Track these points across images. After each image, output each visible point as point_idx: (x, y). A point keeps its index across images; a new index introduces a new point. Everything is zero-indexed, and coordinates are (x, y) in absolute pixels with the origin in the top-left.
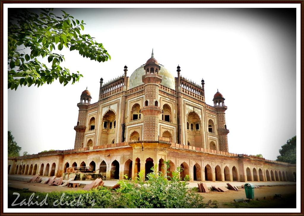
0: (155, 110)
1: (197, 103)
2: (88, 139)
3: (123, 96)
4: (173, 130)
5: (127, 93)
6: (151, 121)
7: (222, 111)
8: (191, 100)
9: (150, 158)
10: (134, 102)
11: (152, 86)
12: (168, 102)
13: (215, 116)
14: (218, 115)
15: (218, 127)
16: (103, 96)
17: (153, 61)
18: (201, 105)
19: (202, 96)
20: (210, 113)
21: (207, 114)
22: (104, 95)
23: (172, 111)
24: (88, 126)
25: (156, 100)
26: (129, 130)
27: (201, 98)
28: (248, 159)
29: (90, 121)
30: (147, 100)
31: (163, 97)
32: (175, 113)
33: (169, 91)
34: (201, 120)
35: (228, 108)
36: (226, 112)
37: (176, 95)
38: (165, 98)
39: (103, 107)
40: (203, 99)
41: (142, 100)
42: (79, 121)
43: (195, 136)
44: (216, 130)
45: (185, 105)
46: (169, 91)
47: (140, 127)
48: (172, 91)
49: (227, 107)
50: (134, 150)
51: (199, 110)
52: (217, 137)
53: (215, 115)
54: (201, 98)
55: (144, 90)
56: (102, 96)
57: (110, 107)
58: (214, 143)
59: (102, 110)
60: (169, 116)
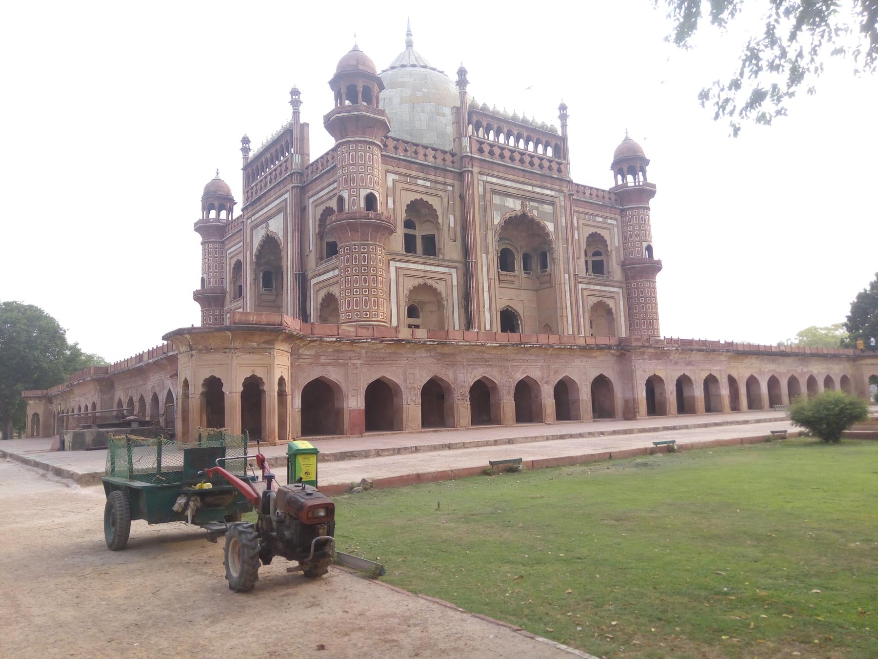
0: (362, 224)
1: (538, 183)
4: (445, 280)
6: (356, 259)
8: (516, 178)
9: (253, 377)
10: (322, 203)
11: (352, 147)
12: (426, 193)
13: (615, 219)
14: (627, 216)
15: (625, 254)
17: (354, 63)
18: (552, 189)
19: (559, 157)
20: (594, 212)
21: (582, 216)
22: (252, 188)
23: (440, 220)
24: (228, 287)
25: (369, 191)
27: (555, 166)
28: (651, 350)
29: (233, 273)
31: (402, 178)
32: (452, 225)
33: (425, 155)
34: (552, 237)
35: (658, 189)
37: (454, 167)
38: (413, 181)
40: (559, 171)
42: (205, 276)
43: (536, 291)
44: (615, 265)
45: (488, 195)
46: (425, 155)
49: (654, 186)
50: (179, 356)
51: (545, 206)
52: (619, 287)
53: (613, 216)
54: (555, 166)
57: (267, 227)
58: (608, 305)
59: (252, 235)
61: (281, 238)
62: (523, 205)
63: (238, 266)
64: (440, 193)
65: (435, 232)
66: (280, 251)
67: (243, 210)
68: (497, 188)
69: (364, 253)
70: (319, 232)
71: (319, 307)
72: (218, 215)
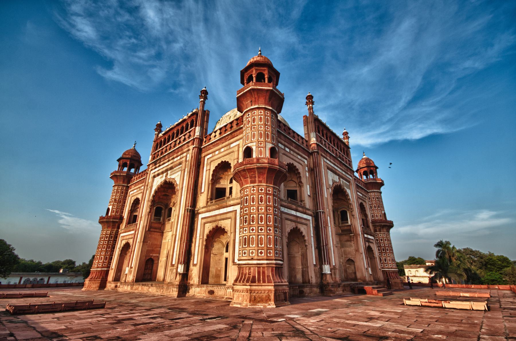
2: (124, 242)
3: (193, 149)
5: (204, 143)
7: (376, 189)
22: (158, 152)
23: (302, 180)
24: (126, 215)
26: (203, 223)
29: (132, 206)
30: (249, 145)
35: (385, 183)
36: (382, 189)
39: (154, 177)
41: (236, 153)
42: (111, 207)
47: (229, 215)
48: (301, 141)
49: (383, 181)
52: (374, 236)
59: (153, 181)
60: (296, 191)
61: (178, 183)
62: (339, 178)
63: (137, 202)
64: (302, 163)
65: (298, 189)
67: (149, 165)
68: (329, 166)
69: (270, 194)
70: (212, 179)
71: (205, 237)
72: (129, 170)
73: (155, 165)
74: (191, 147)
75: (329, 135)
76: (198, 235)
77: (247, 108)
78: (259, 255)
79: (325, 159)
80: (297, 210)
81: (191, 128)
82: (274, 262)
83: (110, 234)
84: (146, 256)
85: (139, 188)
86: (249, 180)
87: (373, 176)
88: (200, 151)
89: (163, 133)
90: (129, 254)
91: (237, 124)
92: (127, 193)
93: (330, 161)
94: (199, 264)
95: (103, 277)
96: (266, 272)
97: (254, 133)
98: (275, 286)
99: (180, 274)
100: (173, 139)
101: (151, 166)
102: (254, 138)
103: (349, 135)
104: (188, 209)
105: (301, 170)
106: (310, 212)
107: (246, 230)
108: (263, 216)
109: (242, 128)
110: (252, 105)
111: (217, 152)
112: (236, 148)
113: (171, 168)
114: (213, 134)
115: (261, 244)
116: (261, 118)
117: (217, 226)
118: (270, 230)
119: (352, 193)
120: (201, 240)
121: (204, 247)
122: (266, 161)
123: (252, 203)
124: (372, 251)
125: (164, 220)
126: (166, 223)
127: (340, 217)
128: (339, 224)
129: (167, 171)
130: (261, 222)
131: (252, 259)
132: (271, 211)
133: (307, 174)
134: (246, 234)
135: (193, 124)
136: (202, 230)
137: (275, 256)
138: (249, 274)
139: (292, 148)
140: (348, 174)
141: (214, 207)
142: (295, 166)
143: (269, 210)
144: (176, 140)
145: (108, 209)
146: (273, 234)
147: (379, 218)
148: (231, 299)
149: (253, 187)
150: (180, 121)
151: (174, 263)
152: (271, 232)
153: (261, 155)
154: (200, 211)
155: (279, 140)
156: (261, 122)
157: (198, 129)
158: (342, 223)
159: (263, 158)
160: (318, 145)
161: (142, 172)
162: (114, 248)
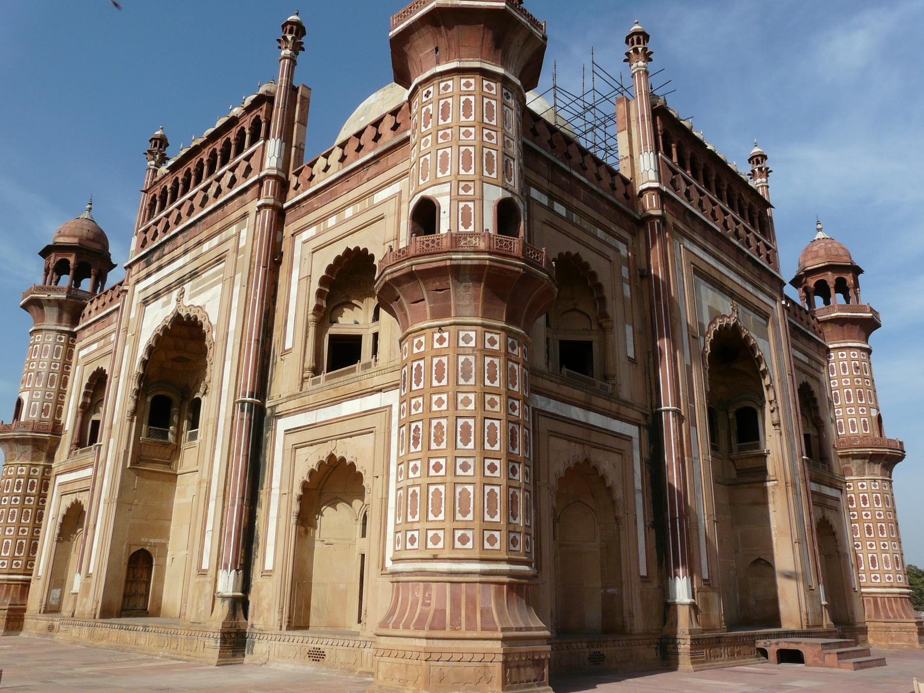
2: (67, 501)
3: (258, 212)
5: (291, 192)
16: (153, 229)
22: (156, 224)
23: (609, 310)
29: (86, 395)
30: (428, 193)
35: (883, 319)
39: (145, 302)
42: (25, 397)
43: (729, 485)
47: (367, 422)
48: (607, 180)
55: (408, 139)
56: (149, 235)
59: (142, 315)
60: (589, 344)
61: (214, 321)
63: (98, 382)
64: (610, 252)
65: (594, 338)
66: (203, 352)
67: (130, 267)
69: (493, 354)
70: (318, 308)
71: (297, 491)
73: (148, 264)
74: (253, 206)
75: (701, 161)
76: (276, 484)
77: (422, 72)
78: (458, 545)
79: (687, 244)
80: (587, 407)
81: (252, 142)
82: (505, 567)
83: (29, 477)
84: (130, 546)
85: (104, 337)
86: (427, 305)
87: (847, 298)
88: (279, 217)
89: (170, 163)
90: (81, 537)
91: (395, 127)
92: (69, 354)
93: (705, 249)
94: (278, 572)
95: (13, 599)
96: (479, 598)
97: (445, 155)
98: (504, 640)
99: (224, 598)
100: (198, 181)
101: (135, 268)
102: (444, 170)
103: (767, 164)
104: (243, 402)
105: (604, 278)
106: (633, 414)
107: (415, 469)
108: (471, 422)
109: (408, 139)
110: (438, 63)
111: (332, 221)
112: (392, 205)
113: (194, 275)
114: (322, 162)
115: (465, 513)
116: (467, 102)
117: (332, 456)
118: (493, 468)
119: (773, 351)
120: (285, 498)
121: (293, 520)
122: (482, 245)
123: (435, 383)
124: (834, 534)
125: (178, 435)
126: (184, 445)
127: (735, 428)
128: (730, 450)
129: (181, 282)
130: (466, 441)
131: (435, 558)
132: (497, 408)
133: (627, 288)
134: (418, 482)
135: (257, 132)
136: (287, 471)
137: (509, 551)
138: (424, 604)
139: (575, 203)
140: (763, 291)
141: (322, 397)
142: (586, 265)
143: (493, 403)
144: (208, 186)
145: (19, 403)
146: (503, 481)
147: (859, 431)
148: (372, 674)
149: (440, 328)
150: (219, 124)
151: (205, 566)
152: (497, 473)
153: (466, 225)
154: (278, 409)
155: (532, 176)
156: (467, 115)
157: (273, 147)
158: (740, 449)
159: (472, 235)
160: (663, 197)
161: (113, 289)
162: (40, 519)
